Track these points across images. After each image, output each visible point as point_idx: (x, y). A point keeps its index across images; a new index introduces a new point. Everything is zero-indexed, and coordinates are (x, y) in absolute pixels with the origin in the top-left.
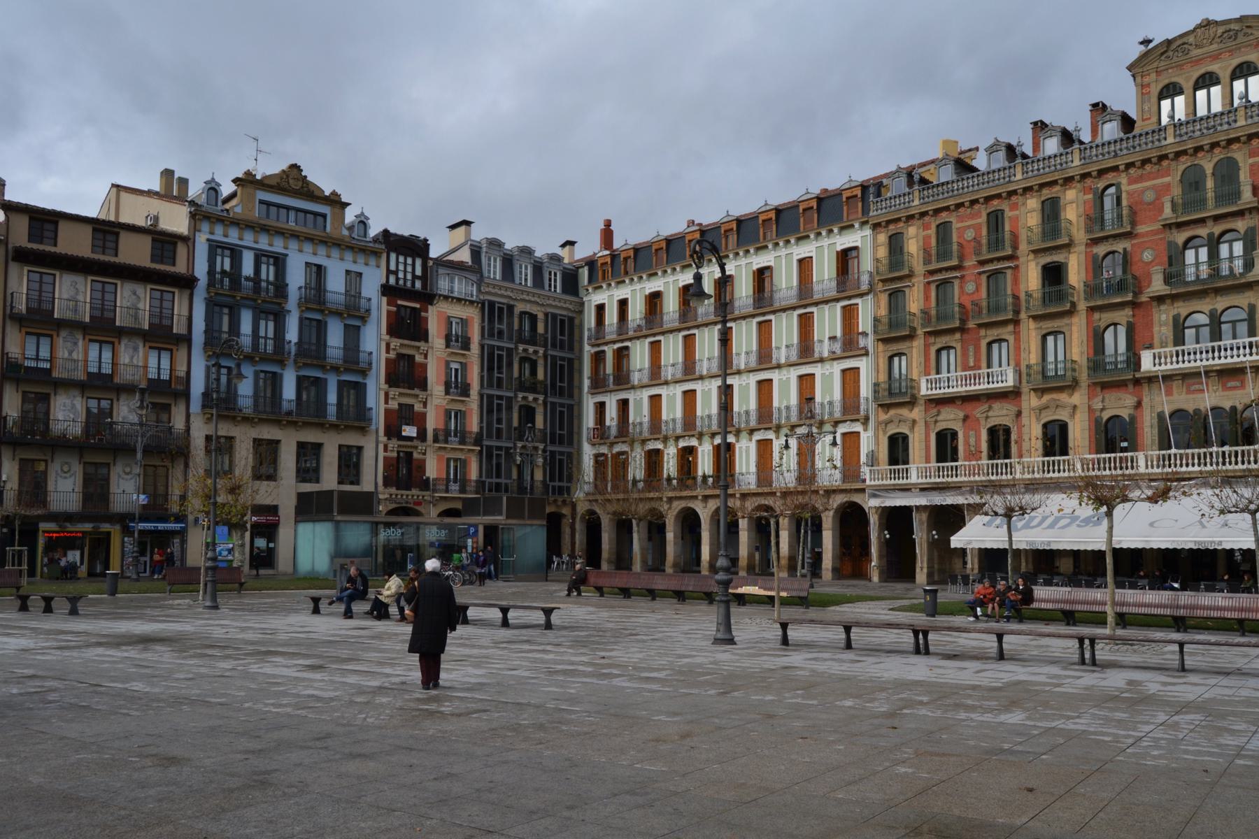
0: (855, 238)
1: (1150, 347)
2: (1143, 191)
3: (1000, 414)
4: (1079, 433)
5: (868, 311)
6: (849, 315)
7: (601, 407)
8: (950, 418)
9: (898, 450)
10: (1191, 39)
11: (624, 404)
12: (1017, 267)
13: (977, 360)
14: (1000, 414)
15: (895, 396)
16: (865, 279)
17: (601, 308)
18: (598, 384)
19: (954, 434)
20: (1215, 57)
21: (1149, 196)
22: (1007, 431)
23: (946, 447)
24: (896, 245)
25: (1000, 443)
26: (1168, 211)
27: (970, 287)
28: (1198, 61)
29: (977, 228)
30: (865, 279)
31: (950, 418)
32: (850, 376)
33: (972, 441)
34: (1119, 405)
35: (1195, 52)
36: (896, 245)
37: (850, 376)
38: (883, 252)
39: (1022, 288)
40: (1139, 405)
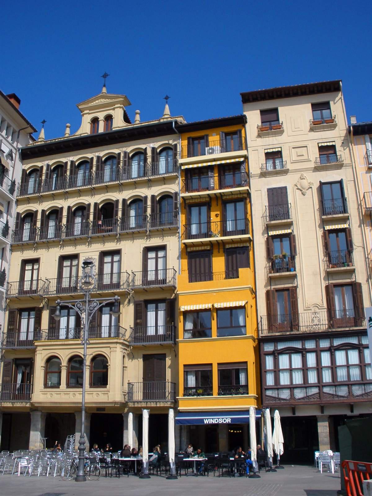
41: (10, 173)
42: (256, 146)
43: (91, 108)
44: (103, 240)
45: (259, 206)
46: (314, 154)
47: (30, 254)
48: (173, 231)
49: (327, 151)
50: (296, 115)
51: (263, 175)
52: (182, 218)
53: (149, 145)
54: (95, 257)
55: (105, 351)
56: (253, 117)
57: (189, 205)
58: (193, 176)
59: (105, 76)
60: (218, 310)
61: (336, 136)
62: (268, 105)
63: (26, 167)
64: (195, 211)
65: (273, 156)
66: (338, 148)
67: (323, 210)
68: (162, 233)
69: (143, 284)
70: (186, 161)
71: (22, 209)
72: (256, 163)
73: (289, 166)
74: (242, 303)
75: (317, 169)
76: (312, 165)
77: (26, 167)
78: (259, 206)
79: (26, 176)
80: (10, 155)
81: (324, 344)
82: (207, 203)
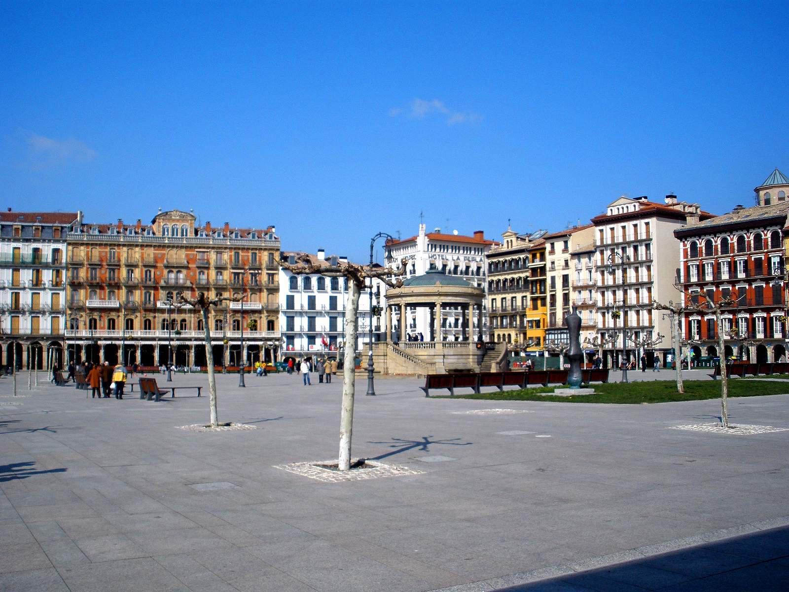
0: (62, 247)
1: (159, 300)
2: (158, 254)
4: (137, 323)
5: (65, 275)
10: (172, 213)
12: (119, 269)
13: (105, 296)
19: (95, 320)
20: (178, 221)
21: (160, 256)
22: (114, 321)
23: (93, 325)
25: (112, 325)
26: (165, 262)
27: (103, 272)
28: (174, 220)
29: (106, 252)
33: (102, 322)
34: (150, 316)
35: (173, 218)
39: (121, 274)
40: (155, 317)
41: (483, 267)
42: (549, 258)
43: (506, 236)
44: (512, 293)
45: (549, 282)
46: (563, 263)
47: (493, 297)
48: (528, 291)
49: (566, 262)
50: (559, 245)
51: (550, 271)
52: (530, 286)
53: (522, 256)
54: (510, 298)
55: (510, 333)
56: (548, 246)
57: (532, 282)
58: (534, 271)
59: (509, 220)
60: (535, 321)
61: (567, 256)
62: (552, 241)
63: (489, 261)
64: (534, 284)
65: (553, 263)
66: (569, 261)
67: (564, 286)
68: (526, 291)
69: (522, 309)
70: (530, 265)
71: (490, 279)
72: (548, 266)
73: (556, 268)
74: (539, 319)
75: (563, 269)
76: (562, 268)
77: (489, 261)
78: (549, 282)
79: (490, 265)
80: (481, 260)
81: (559, 332)
82: (536, 281)
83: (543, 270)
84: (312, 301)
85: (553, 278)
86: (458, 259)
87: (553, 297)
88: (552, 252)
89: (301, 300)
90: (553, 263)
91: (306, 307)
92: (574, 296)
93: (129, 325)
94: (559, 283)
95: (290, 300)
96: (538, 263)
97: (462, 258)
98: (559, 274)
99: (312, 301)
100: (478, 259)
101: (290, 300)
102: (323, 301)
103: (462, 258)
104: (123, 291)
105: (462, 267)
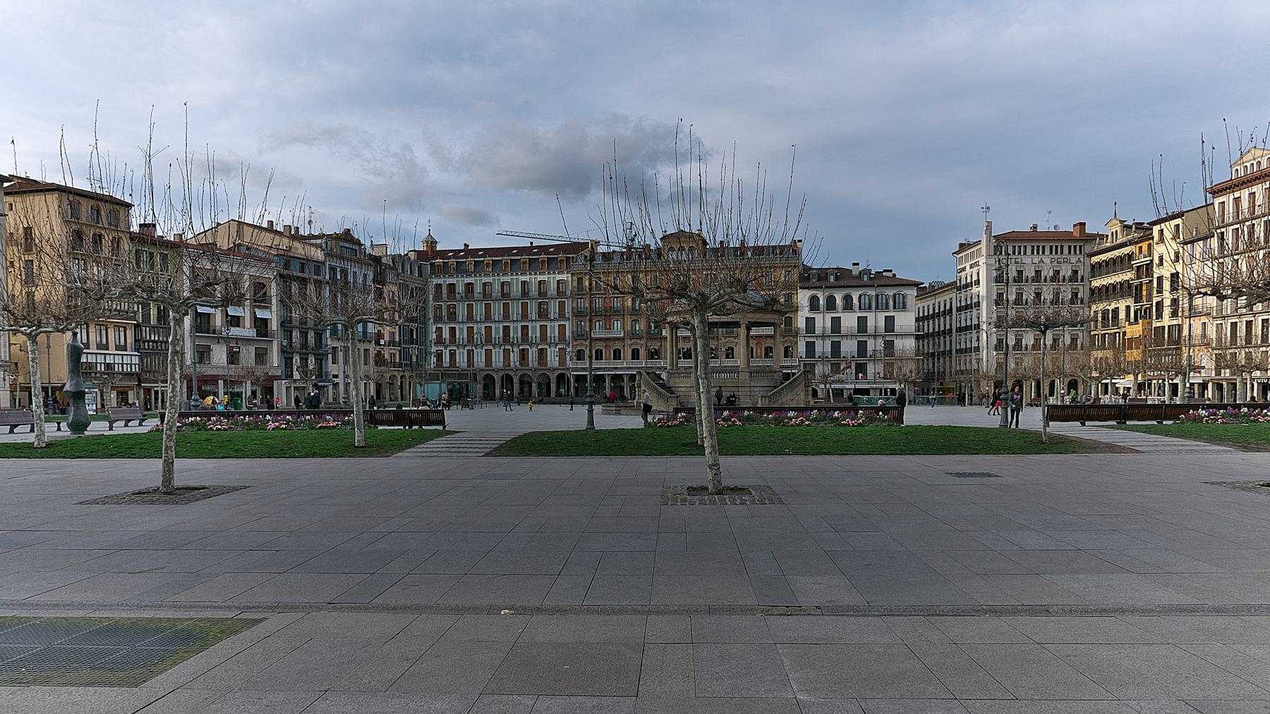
3: (617, 345)
4: (642, 353)
6: (562, 305)
7: (439, 330)
8: (600, 345)
9: (580, 355)
11: (453, 330)
14: (617, 345)
15: (578, 336)
16: (568, 293)
17: (439, 286)
18: (438, 319)
24: (580, 280)
30: (568, 293)
31: (600, 345)
32: (562, 328)
36: (580, 280)
37: (562, 328)
38: (575, 284)
65: (1161, 259)
83: (1149, 266)
84: (836, 322)
85: (1160, 279)
86: (1042, 261)
87: (1160, 305)
88: (1162, 240)
89: (823, 321)
90: (1161, 259)
91: (829, 331)
92: (1184, 303)
93: (635, 354)
94: (1167, 285)
95: (810, 322)
96: (1143, 260)
97: (1047, 260)
98: (1166, 271)
99: (836, 322)
100: (1074, 260)
101: (810, 322)
102: (849, 321)
103: (1047, 260)
104: (628, 320)
105: (1047, 272)
